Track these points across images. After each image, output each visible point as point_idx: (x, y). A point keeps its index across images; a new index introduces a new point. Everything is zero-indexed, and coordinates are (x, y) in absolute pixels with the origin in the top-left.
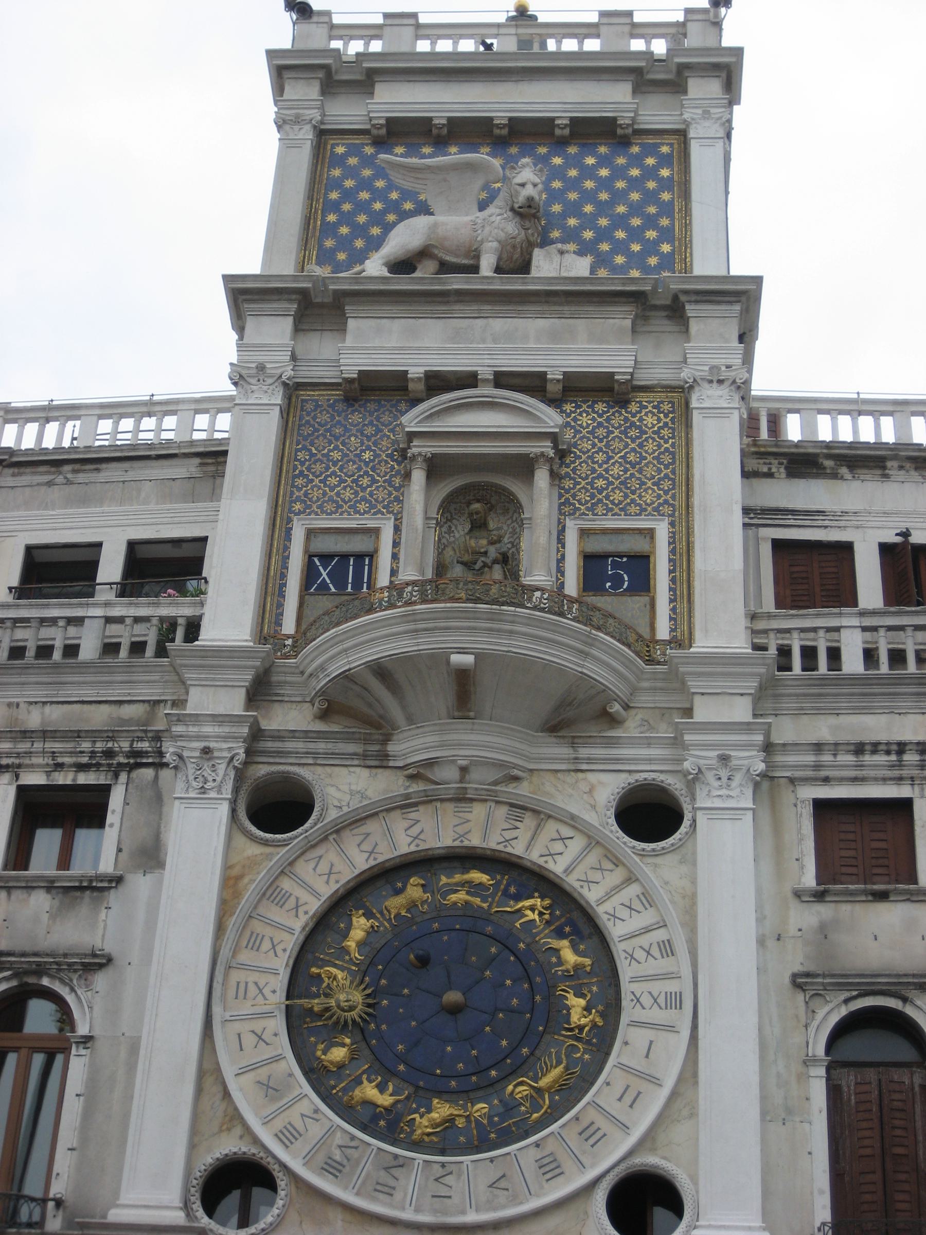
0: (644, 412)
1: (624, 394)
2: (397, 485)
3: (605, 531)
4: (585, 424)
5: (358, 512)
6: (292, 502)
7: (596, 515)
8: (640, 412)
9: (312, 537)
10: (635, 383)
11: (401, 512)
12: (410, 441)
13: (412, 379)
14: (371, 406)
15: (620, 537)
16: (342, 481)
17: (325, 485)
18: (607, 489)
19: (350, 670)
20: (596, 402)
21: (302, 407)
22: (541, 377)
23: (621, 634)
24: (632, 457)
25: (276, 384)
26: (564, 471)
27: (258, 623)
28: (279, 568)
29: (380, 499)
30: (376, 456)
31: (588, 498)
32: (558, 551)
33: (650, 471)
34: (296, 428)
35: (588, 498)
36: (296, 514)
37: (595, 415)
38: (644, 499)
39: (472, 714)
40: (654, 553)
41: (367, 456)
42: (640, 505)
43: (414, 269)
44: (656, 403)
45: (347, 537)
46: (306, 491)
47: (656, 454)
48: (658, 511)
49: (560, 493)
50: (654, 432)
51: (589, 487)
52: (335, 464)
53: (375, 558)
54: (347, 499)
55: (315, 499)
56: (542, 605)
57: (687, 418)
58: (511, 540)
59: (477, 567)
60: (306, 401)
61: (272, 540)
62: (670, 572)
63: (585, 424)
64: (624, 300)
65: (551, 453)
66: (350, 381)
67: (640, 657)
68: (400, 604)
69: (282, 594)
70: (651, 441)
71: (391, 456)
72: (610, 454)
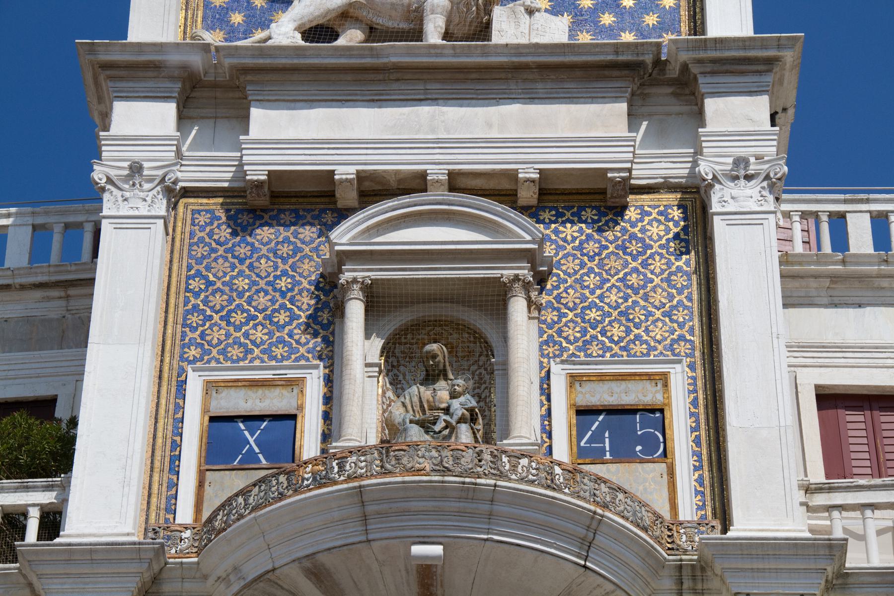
0: (647, 219)
1: (621, 197)
2: (325, 321)
3: (602, 378)
4: (569, 238)
5: (274, 358)
7: (590, 355)
10: (633, 182)
12: (341, 263)
13: (341, 181)
15: (624, 385)
17: (229, 323)
19: (274, 570)
20: (582, 208)
21: (193, 219)
22: (512, 175)
23: (634, 514)
24: (634, 279)
25: (159, 188)
26: (544, 299)
28: (169, 434)
29: (303, 340)
31: (578, 335)
32: (542, 405)
33: (658, 297)
34: (186, 248)
35: (578, 335)
36: (190, 362)
40: (669, 405)
41: (283, 284)
42: (646, 342)
43: (335, 36)
44: (662, 208)
45: (260, 391)
46: (203, 332)
48: (673, 350)
50: (661, 246)
51: (579, 320)
52: (240, 295)
53: (299, 419)
55: (215, 341)
56: (530, 477)
59: (437, 428)
60: (199, 212)
61: (158, 397)
63: (569, 238)
64: (616, 73)
66: (259, 184)
67: (660, 544)
68: (342, 478)
69: (175, 470)
70: (657, 258)
72: (605, 276)
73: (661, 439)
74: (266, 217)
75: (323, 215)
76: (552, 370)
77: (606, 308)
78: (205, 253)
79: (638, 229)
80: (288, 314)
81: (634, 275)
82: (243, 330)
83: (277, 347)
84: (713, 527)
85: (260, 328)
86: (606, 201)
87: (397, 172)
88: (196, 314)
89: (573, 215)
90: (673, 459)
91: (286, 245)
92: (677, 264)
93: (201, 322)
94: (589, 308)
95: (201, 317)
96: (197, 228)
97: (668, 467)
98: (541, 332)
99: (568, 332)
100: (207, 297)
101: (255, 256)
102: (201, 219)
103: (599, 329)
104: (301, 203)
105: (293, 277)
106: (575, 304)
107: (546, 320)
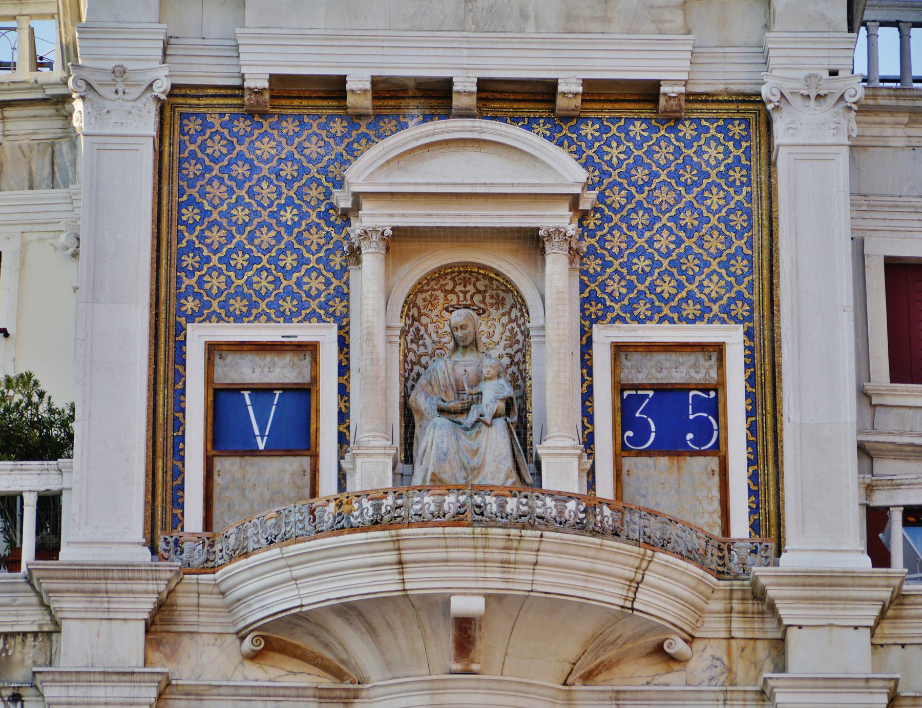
2: (338, 267)
3: (650, 348)
5: (283, 314)
6: (179, 296)
8: (697, 138)
9: (217, 358)
11: (347, 315)
14: (289, 126)
15: (673, 357)
16: (254, 261)
18: (651, 274)
19: (302, 606)
21: (182, 126)
22: (552, 85)
24: (688, 219)
25: (144, 99)
27: (146, 503)
29: (314, 292)
30: (303, 216)
31: (624, 291)
32: (583, 381)
34: (176, 164)
37: (631, 145)
38: (707, 291)
39: (475, 667)
41: (288, 215)
44: (721, 123)
47: (723, 213)
49: (582, 282)
51: (624, 271)
52: (241, 228)
53: (314, 394)
54: (264, 291)
55: (215, 291)
57: (769, 152)
58: (509, 350)
62: (749, 414)
65: (572, 229)
70: (715, 190)
71: (324, 216)
73: (715, 427)
74: (266, 125)
75: (332, 124)
76: (595, 338)
77: (657, 257)
78: (198, 173)
79: (694, 149)
80: (295, 256)
81: (688, 213)
82: (246, 277)
83: (285, 300)
84: (767, 546)
85: (264, 274)
86: (657, 112)
87: (416, 78)
88: (191, 255)
89: (619, 129)
90: (726, 452)
91: (290, 164)
92: (737, 198)
93: (197, 265)
94: (636, 255)
95: (197, 258)
96: (187, 138)
97: (720, 463)
98: (583, 286)
99: (612, 286)
100: (202, 231)
101: (256, 177)
102: (191, 125)
103: (647, 283)
104: (305, 107)
105: (299, 207)
106: (620, 249)
107: (587, 270)
